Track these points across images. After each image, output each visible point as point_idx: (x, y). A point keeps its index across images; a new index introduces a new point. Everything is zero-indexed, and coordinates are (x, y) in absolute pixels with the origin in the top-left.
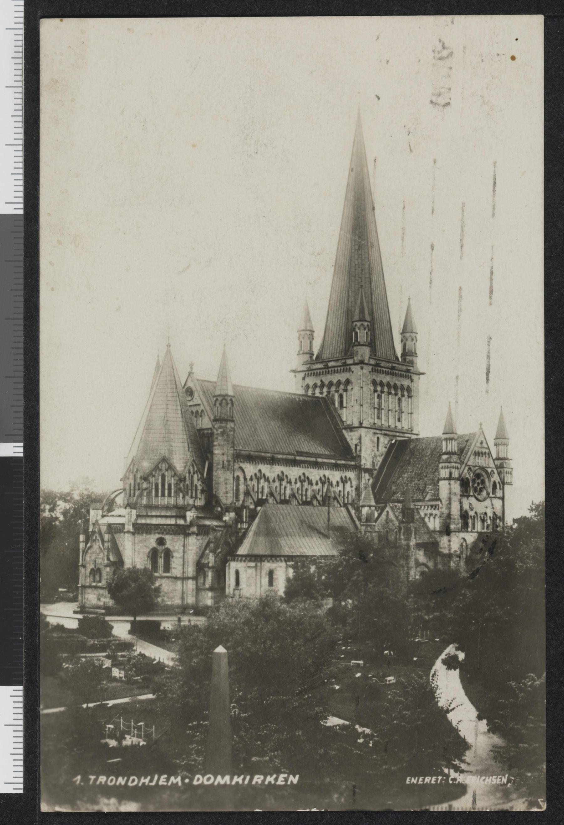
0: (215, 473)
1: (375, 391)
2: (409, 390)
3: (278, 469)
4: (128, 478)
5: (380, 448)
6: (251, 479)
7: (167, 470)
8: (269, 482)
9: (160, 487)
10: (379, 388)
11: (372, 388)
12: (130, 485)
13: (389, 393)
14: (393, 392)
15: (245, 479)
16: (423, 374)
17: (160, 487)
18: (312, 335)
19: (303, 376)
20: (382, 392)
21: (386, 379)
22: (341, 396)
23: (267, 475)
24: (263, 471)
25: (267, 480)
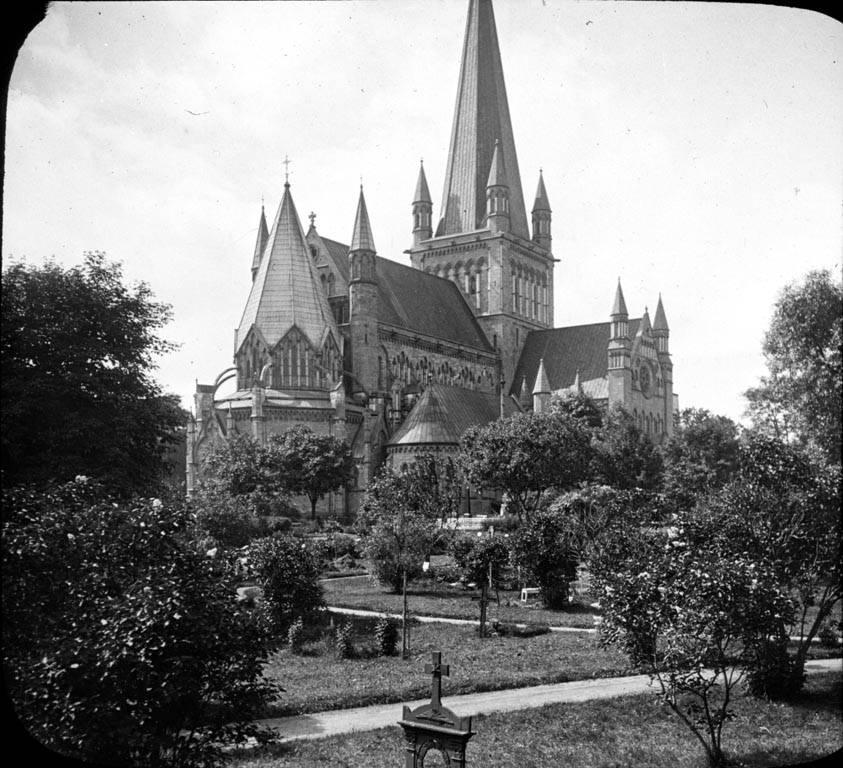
0: (355, 351)
1: (513, 273)
2: (544, 278)
3: (422, 353)
4: (245, 354)
5: (519, 342)
6: (394, 363)
7: (298, 341)
8: (412, 368)
9: (290, 363)
10: (517, 272)
11: (510, 270)
12: (248, 362)
13: (526, 279)
14: (530, 278)
15: (388, 361)
16: (558, 261)
17: (290, 363)
18: (431, 208)
19: (420, 258)
20: (520, 276)
21: (525, 260)
22: (473, 279)
23: (410, 359)
24: (406, 353)
25: (410, 365)
